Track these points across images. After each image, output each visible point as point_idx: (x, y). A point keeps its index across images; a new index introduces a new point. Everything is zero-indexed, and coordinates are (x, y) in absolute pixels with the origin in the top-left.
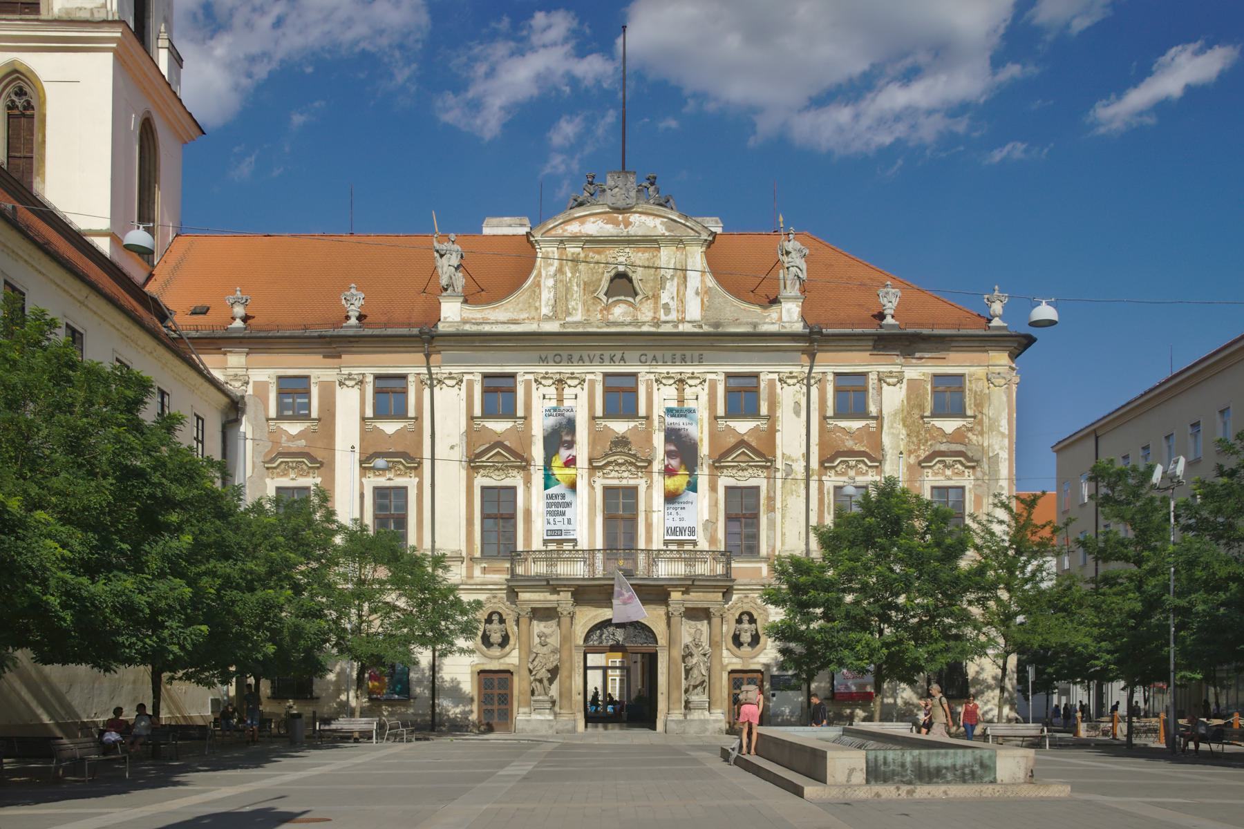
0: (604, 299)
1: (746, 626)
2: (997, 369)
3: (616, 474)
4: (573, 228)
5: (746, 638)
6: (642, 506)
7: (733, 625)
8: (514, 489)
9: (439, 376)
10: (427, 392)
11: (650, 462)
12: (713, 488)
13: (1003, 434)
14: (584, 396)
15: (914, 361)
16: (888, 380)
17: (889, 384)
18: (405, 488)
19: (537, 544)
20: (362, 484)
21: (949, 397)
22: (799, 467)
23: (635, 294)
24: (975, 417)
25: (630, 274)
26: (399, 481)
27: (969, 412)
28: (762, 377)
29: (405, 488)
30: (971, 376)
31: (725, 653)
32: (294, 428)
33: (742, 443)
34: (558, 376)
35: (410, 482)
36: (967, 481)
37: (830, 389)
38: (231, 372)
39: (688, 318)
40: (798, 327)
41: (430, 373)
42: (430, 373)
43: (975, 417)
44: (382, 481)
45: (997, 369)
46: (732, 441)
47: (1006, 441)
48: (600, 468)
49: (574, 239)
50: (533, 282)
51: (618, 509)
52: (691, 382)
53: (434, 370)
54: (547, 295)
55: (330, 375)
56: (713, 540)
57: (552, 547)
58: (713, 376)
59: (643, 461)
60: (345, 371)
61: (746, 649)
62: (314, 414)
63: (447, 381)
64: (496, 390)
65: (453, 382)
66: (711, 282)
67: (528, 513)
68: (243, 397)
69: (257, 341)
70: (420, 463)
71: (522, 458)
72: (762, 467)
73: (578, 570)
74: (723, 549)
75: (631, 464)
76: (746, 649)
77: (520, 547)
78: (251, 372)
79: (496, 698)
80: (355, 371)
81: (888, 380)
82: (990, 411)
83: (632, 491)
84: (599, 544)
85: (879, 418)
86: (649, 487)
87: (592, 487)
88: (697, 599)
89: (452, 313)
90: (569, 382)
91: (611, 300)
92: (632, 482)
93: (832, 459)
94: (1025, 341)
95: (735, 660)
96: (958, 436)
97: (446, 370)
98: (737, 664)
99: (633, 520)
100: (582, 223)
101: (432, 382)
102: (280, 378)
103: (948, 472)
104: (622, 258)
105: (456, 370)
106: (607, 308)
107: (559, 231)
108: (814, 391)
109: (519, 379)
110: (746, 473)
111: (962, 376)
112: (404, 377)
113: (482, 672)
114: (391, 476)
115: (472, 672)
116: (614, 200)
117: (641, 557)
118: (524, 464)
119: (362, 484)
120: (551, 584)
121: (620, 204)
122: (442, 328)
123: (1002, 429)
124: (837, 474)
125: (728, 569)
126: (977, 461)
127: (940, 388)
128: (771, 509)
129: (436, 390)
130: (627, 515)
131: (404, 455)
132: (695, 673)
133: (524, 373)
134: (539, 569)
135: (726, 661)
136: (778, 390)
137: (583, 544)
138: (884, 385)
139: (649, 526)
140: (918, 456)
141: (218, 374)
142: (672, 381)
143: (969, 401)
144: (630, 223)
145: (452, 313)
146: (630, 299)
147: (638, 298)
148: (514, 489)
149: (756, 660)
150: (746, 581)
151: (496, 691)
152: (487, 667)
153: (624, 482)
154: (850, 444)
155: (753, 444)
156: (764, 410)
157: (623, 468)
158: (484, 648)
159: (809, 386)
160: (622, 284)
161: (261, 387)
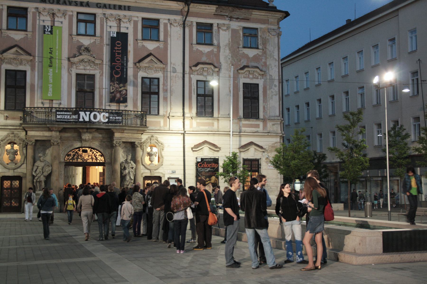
2: (272, 27)
3: (82, 67)
6: (97, 85)
8: (25, 72)
13: (276, 59)
15: (234, 20)
17: (223, 30)
22: (179, 69)
27: (260, 47)
28: (161, 21)
30: (261, 28)
31: (142, 166)
33: (150, 55)
51: (84, 87)
58: (136, 19)
67: (33, 86)
77: (28, 105)
83: (92, 77)
85: (219, 47)
86: (102, 75)
92: (92, 72)
93: (196, 65)
94: (285, 15)
95: (147, 171)
96: (256, 58)
99: (92, 92)
108: (187, 30)
111: (257, 29)
135: (142, 171)
148: (25, 72)
149: (157, 171)
153: (87, 72)
154: (204, 59)
156: (162, 37)
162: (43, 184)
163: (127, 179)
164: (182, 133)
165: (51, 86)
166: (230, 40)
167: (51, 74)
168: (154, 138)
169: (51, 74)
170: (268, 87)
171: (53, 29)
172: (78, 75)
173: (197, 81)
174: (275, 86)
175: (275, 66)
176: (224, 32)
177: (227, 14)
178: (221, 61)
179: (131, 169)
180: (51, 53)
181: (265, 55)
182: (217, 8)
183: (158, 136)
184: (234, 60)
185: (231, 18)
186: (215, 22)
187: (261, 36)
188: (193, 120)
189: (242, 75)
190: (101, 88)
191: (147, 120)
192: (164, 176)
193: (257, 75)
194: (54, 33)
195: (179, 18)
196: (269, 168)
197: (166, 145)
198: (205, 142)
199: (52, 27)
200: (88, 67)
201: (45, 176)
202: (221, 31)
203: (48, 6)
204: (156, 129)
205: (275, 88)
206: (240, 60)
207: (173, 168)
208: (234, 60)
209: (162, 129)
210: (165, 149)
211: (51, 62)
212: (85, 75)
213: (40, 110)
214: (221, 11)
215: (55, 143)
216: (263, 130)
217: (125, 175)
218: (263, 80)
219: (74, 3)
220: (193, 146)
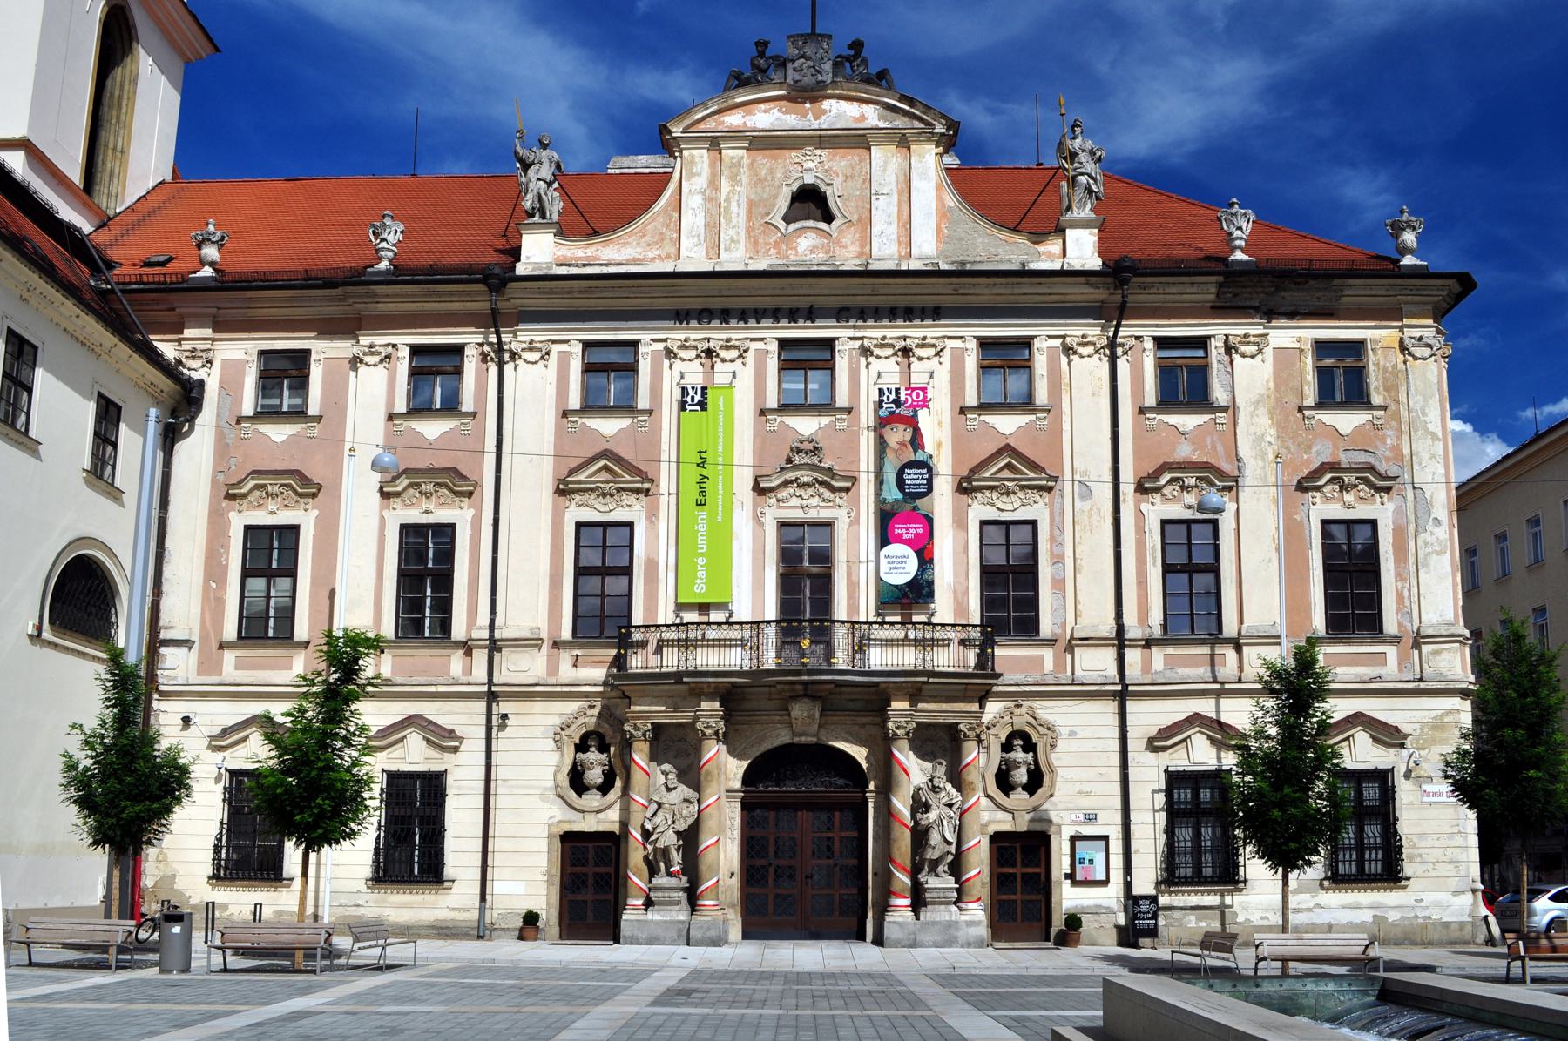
0: (782, 225)
1: (1019, 755)
2: (1417, 333)
3: (795, 501)
4: (734, 120)
5: (1021, 776)
6: (841, 555)
7: (996, 754)
8: (630, 525)
9: (513, 346)
10: (494, 370)
11: (855, 480)
12: (960, 522)
13: (1434, 435)
14: (746, 375)
16: (1243, 349)
17: (1243, 356)
18: (452, 526)
19: (665, 615)
20: (382, 519)
21: (1342, 378)
23: (828, 218)
24: (1385, 408)
25: (823, 188)
26: (441, 515)
27: (1377, 399)
29: (452, 526)
30: (1375, 342)
31: (984, 801)
32: (279, 433)
33: (1007, 449)
34: (705, 345)
35: (458, 515)
37: (1149, 364)
38: (187, 345)
40: (1095, 263)
43: (1385, 408)
44: (415, 516)
45: (1417, 333)
46: (992, 449)
48: (771, 490)
49: (735, 135)
50: (669, 203)
51: (801, 560)
53: (505, 338)
54: (694, 218)
55: (341, 348)
56: (961, 607)
57: (691, 617)
59: (845, 478)
60: (365, 341)
61: (1019, 796)
62: (313, 410)
63: (526, 355)
64: (606, 368)
65: (536, 356)
66: (951, 200)
67: (652, 565)
68: (201, 383)
69: (232, 299)
72: (1040, 488)
73: (735, 659)
75: (823, 484)
76: (1019, 796)
78: (218, 345)
79: (591, 880)
80: (379, 340)
81: (1243, 349)
84: (771, 613)
85: (1230, 409)
86: (855, 522)
87: (758, 521)
88: (934, 711)
89: (540, 251)
90: (723, 354)
91: (792, 227)
92: (825, 514)
95: (1001, 815)
97: (524, 337)
98: (1004, 823)
100: (750, 113)
101: (500, 356)
102: (262, 353)
104: (812, 167)
105: (539, 337)
107: (711, 124)
108: (1123, 365)
109: (642, 349)
110: (1013, 498)
111: (1360, 344)
112: (458, 350)
113: (568, 838)
114: (431, 507)
115: (550, 836)
116: (797, 76)
117: (841, 636)
118: (644, 486)
119: (382, 519)
120: (690, 685)
121: (808, 80)
123: (1431, 427)
124: (1165, 498)
125: (984, 660)
126: (1394, 478)
127: (1328, 362)
128: (1058, 559)
129: (508, 368)
130: (815, 569)
131: (454, 472)
132: (935, 838)
134: (671, 660)
137: (743, 612)
139: (853, 587)
141: (168, 350)
143: (1374, 380)
144: (824, 112)
145: (540, 251)
146: (823, 225)
147: (835, 224)
148: (630, 525)
151: (591, 870)
153: (812, 515)
154: (1184, 452)
155: (1025, 451)
157: (811, 491)
159: (1113, 360)
160: (811, 202)
161: (232, 371)
162: (676, 857)
163: (933, 843)
164: (1114, 694)
165: (701, 561)
166: (1272, 385)
167: (702, 528)
168: (1023, 710)
169: (702, 528)
171: (709, 396)
172: (783, 525)
173: (1164, 522)
174: (1437, 522)
175: (1433, 457)
178: (1241, 454)
179: (947, 810)
180: (701, 465)
181: (1394, 424)
182: (1221, 285)
183: (1037, 704)
184: (1288, 448)
185: (1270, 314)
186: (1218, 331)
187: (1377, 365)
188: (1154, 650)
190: (852, 563)
191: (997, 652)
192: (1059, 833)
194: (709, 406)
195: (1093, 331)
196: (1426, 799)
197: (1064, 731)
198: (1195, 719)
199: (704, 389)
200: (815, 501)
201: (678, 833)
203: (694, 333)
205: (1436, 530)
206: (1310, 447)
207: (1087, 804)
208: (1288, 448)
209: (1050, 680)
210: (1061, 744)
211: (703, 491)
212: (801, 524)
213: (667, 635)
214: (1235, 295)
215: (708, 732)
216: (1400, 670)
217: (927, 829)
218: (1390, 507)
220: (1153, 732)
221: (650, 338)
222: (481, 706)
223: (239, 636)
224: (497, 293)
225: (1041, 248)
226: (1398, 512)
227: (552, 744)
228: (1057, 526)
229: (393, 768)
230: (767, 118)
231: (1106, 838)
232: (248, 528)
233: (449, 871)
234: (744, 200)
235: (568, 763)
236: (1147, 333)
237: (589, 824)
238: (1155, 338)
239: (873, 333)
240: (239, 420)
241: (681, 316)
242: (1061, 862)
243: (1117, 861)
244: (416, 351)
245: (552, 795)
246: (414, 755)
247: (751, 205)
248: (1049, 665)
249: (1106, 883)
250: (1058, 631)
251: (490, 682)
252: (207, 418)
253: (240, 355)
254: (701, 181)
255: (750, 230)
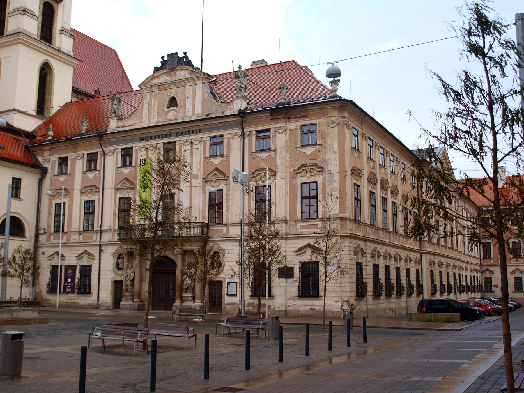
0: (165, 109)
10: (103, 158)
15: (293, 120)
26: (92, 198)
33: (217, 169)
34: (146, 146)
35: (96, 197)
36: (319, 179)
37: (254, 138)
39: (196, 114)
41: (103, 151)
42: (103, 151)
44: (87, 198)
46: (213, 168)
47: (337, 156)
52: (196, 143)
56: (203, 217)
60: (78, 153)
70: (100, 189)
71: (133, 184)
74: (207, 222)
82: (329, 141)
96: (313, 156)
100: (159, 78)
101: (104, 154)
103: (309, 175)
104: (172, 92)
106: (167, 113)
107: (150, 83)
108: (247, 140)
109: (134, 149)
122: (109, 131)
128: (228, 201)
129: (106, 157)
133: (135, 145)
136: (231, 142)
138: (277, 134)
140: (295, 167)
142: (188, 143)
145: (113, 125)
146: (175, 108)
150: (217, 236)
152: (117, 279)
158: (116, 270)
170: (327, 183)
175: (335, 160)
176: (281, 135)
177: (284, 116)
183: (220, 243)
189: (300, 175)
191: (210, 229)
193: (315, 172)
195: (239, 131)
202: (278, 135)
204: (220, 236)
210: (226, 255)
218: (321, 177)
219: (161, 137)
221: (135, 145)
222: (98, 248)
223: (54, 232)
224: (101, 136)
225: (228, 107)
226: (324, 178)
227: (112, 257)
228: (228, 190)
229: (81, 264)
230: (164, 79)
231: (236, 283)
232: (56, 204)
233: (92, 291)
234: (157, 104)
235: (116, 262)
236: (254, 129)
237: (119, 279)
238: (256, 131)
239: (185, 138)
240: (55, 176)
241: (142, 140)
242: (225, 290)
243: (239, 289)
244: (88, 154)
245: (112, 271)
246: (85, 261)
247: (159, 104)
248: (224, 232)
249: (236, 295)
250: (227, 222)
251: (100, 241)
252: (48, 176)
253: (54, 159)
254: (148, 100)
255: (158, 112)
